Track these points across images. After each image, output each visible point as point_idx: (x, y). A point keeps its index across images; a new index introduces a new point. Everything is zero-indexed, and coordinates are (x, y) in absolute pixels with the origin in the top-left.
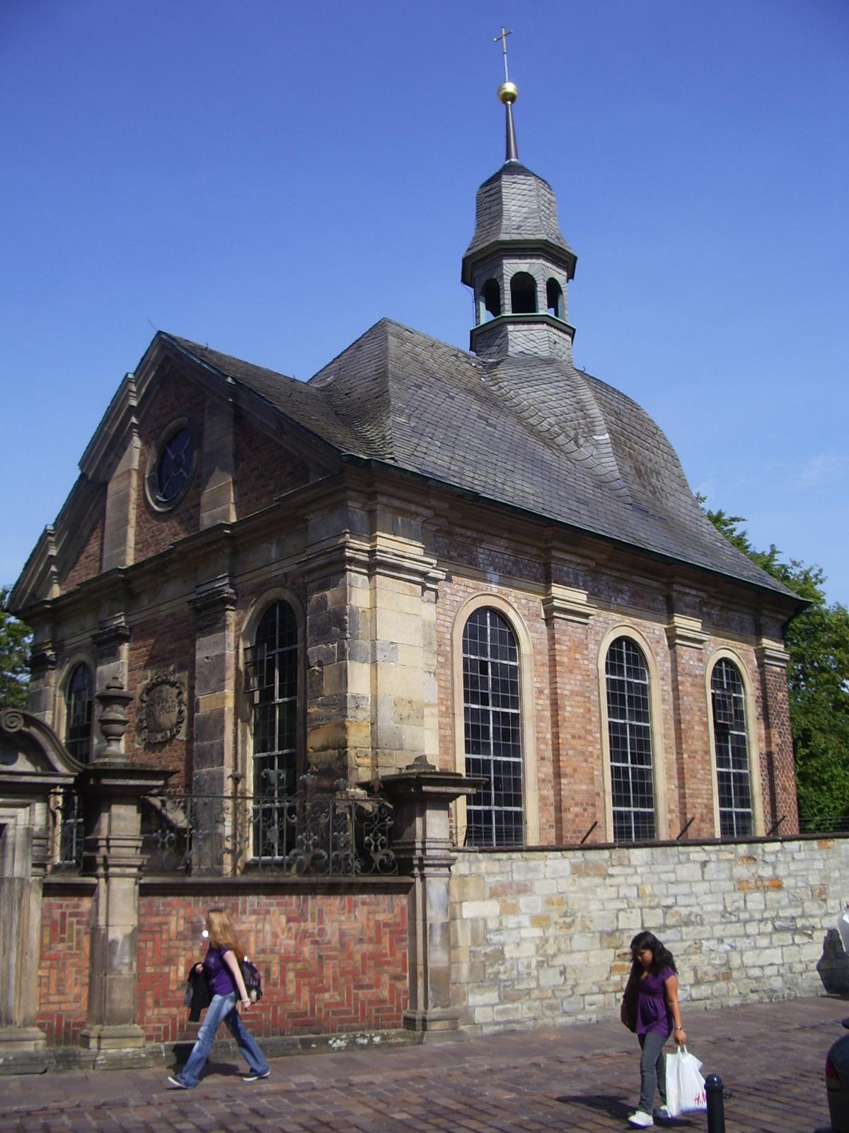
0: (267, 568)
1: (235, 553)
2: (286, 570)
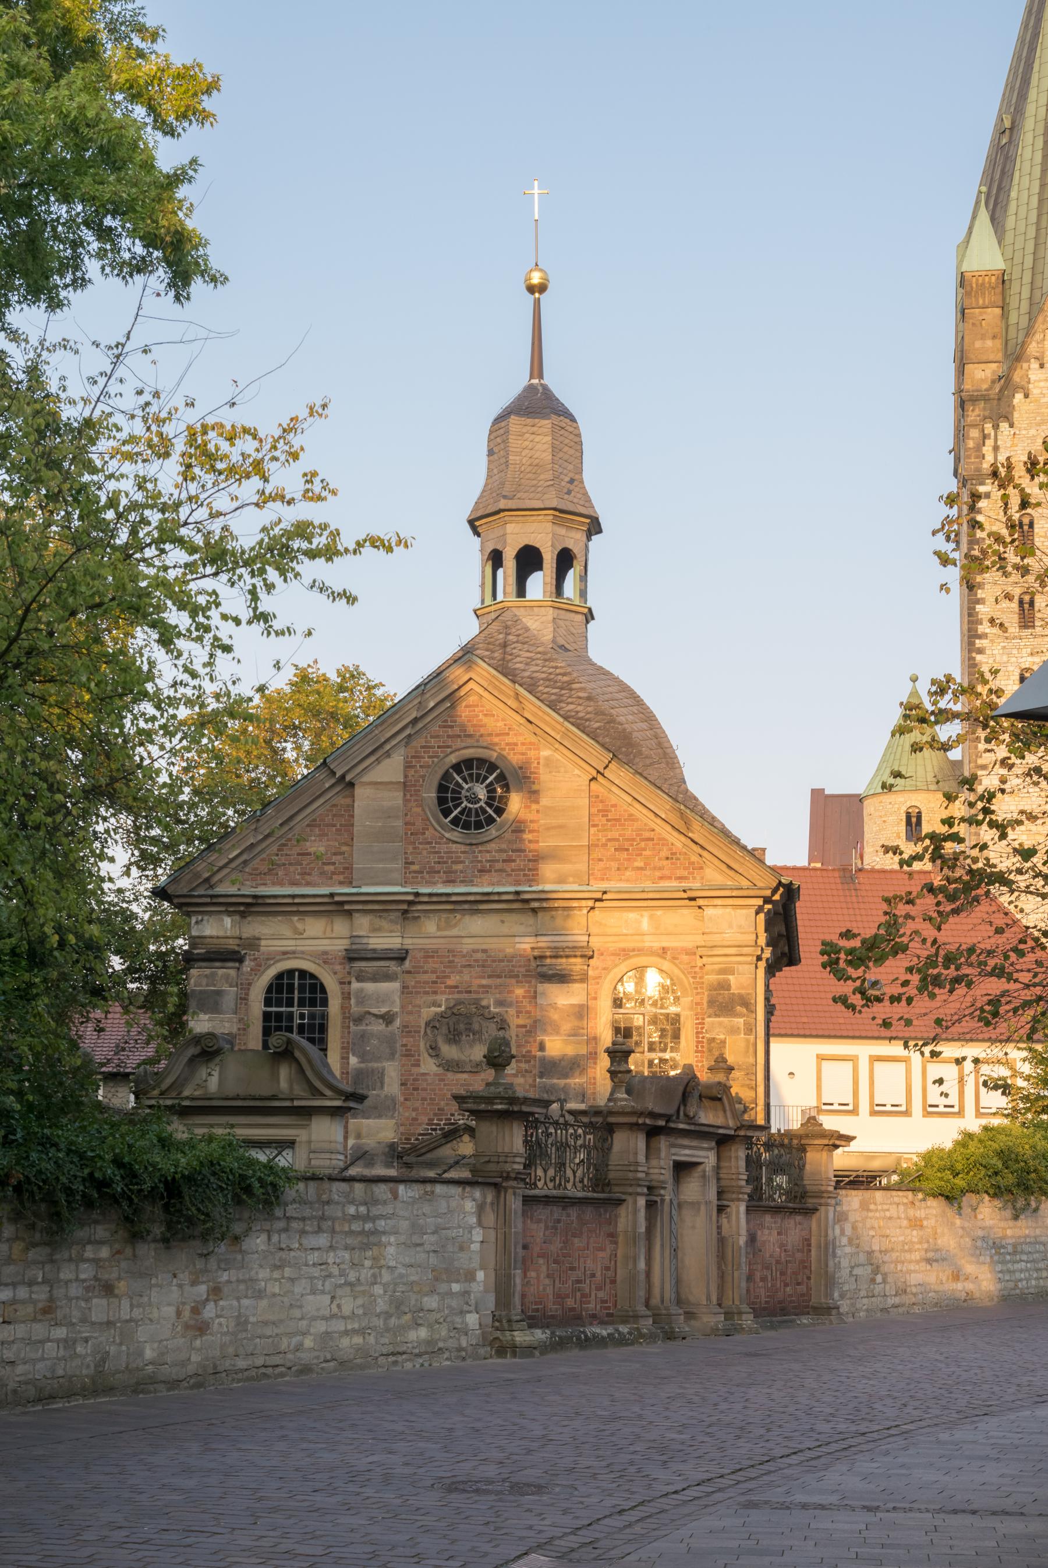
2: (665, 944)
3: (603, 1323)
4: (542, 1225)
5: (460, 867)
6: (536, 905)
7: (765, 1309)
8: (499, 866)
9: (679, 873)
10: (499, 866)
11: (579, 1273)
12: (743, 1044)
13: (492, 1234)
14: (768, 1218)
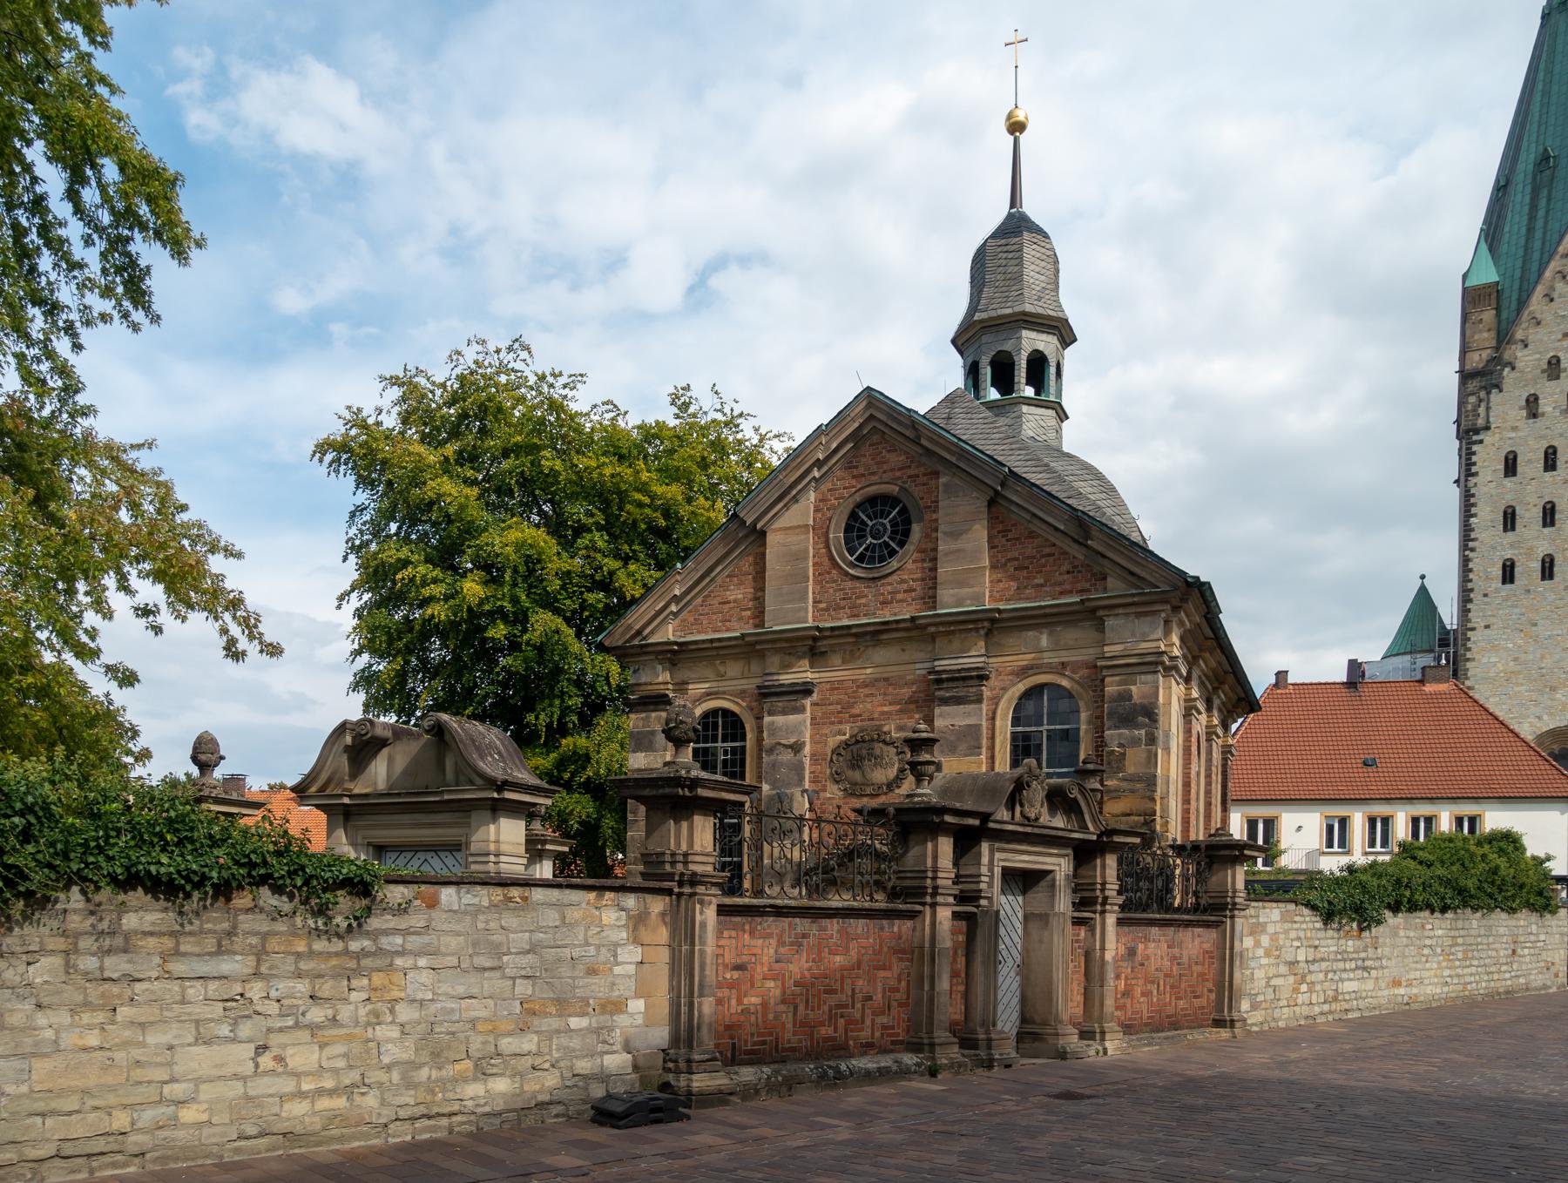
1: (989, 634)
3: (884, 1051)
4: (773, 942)
5: (863, 601)
6: (932, 629)
7: (1146, 1025)
8: (900, 596)
9: (1079, 586)
10: (900, 596)
11: (842, 998)
12: (1144, 755)
13: (664, 955)
14: (1154, 930)
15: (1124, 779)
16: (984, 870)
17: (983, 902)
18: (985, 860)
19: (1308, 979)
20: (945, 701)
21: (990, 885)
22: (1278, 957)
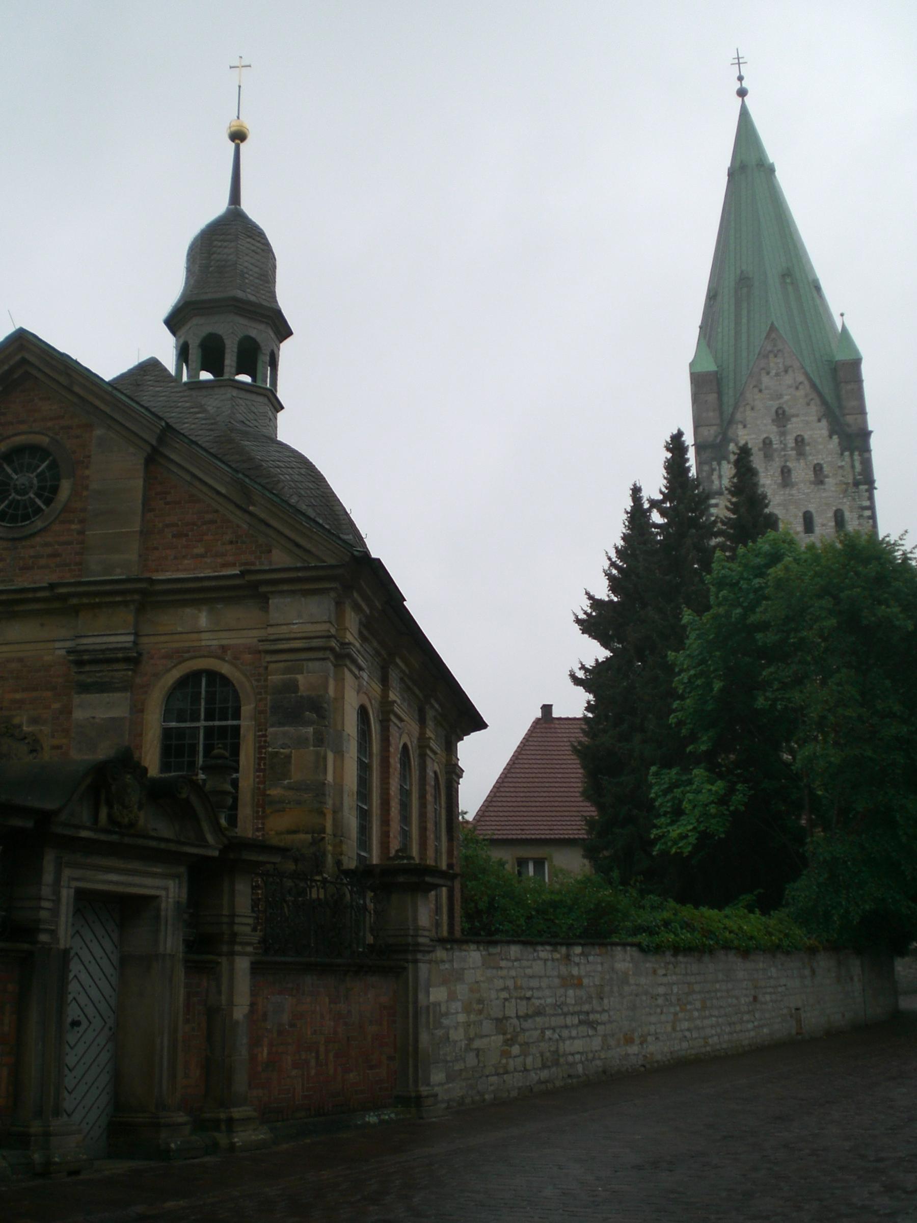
0: (195, 636)
2: (225, 642)
6: (75, 601)
15: (289, 788)
16: (46, 891)
17: (44, 938)
18: (48, 877)
19: (521, 1039)
20: (85, 688)
21: (55, 912)
22: (480, 1012)
